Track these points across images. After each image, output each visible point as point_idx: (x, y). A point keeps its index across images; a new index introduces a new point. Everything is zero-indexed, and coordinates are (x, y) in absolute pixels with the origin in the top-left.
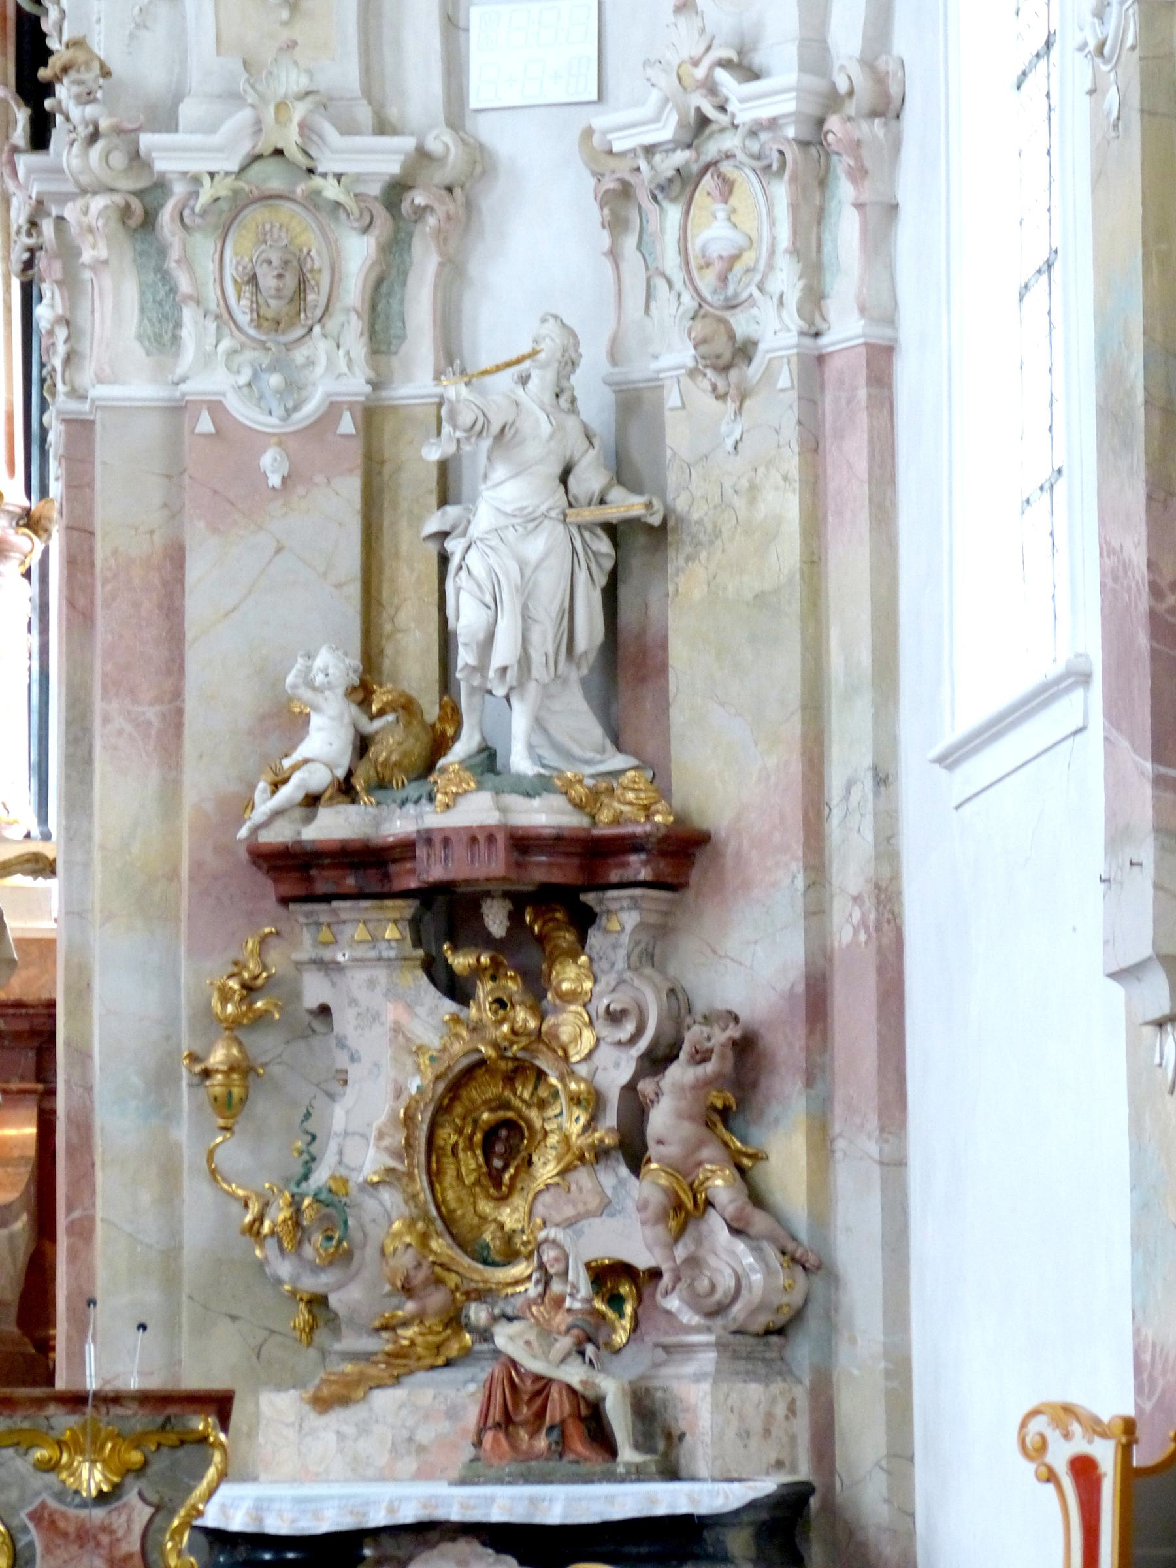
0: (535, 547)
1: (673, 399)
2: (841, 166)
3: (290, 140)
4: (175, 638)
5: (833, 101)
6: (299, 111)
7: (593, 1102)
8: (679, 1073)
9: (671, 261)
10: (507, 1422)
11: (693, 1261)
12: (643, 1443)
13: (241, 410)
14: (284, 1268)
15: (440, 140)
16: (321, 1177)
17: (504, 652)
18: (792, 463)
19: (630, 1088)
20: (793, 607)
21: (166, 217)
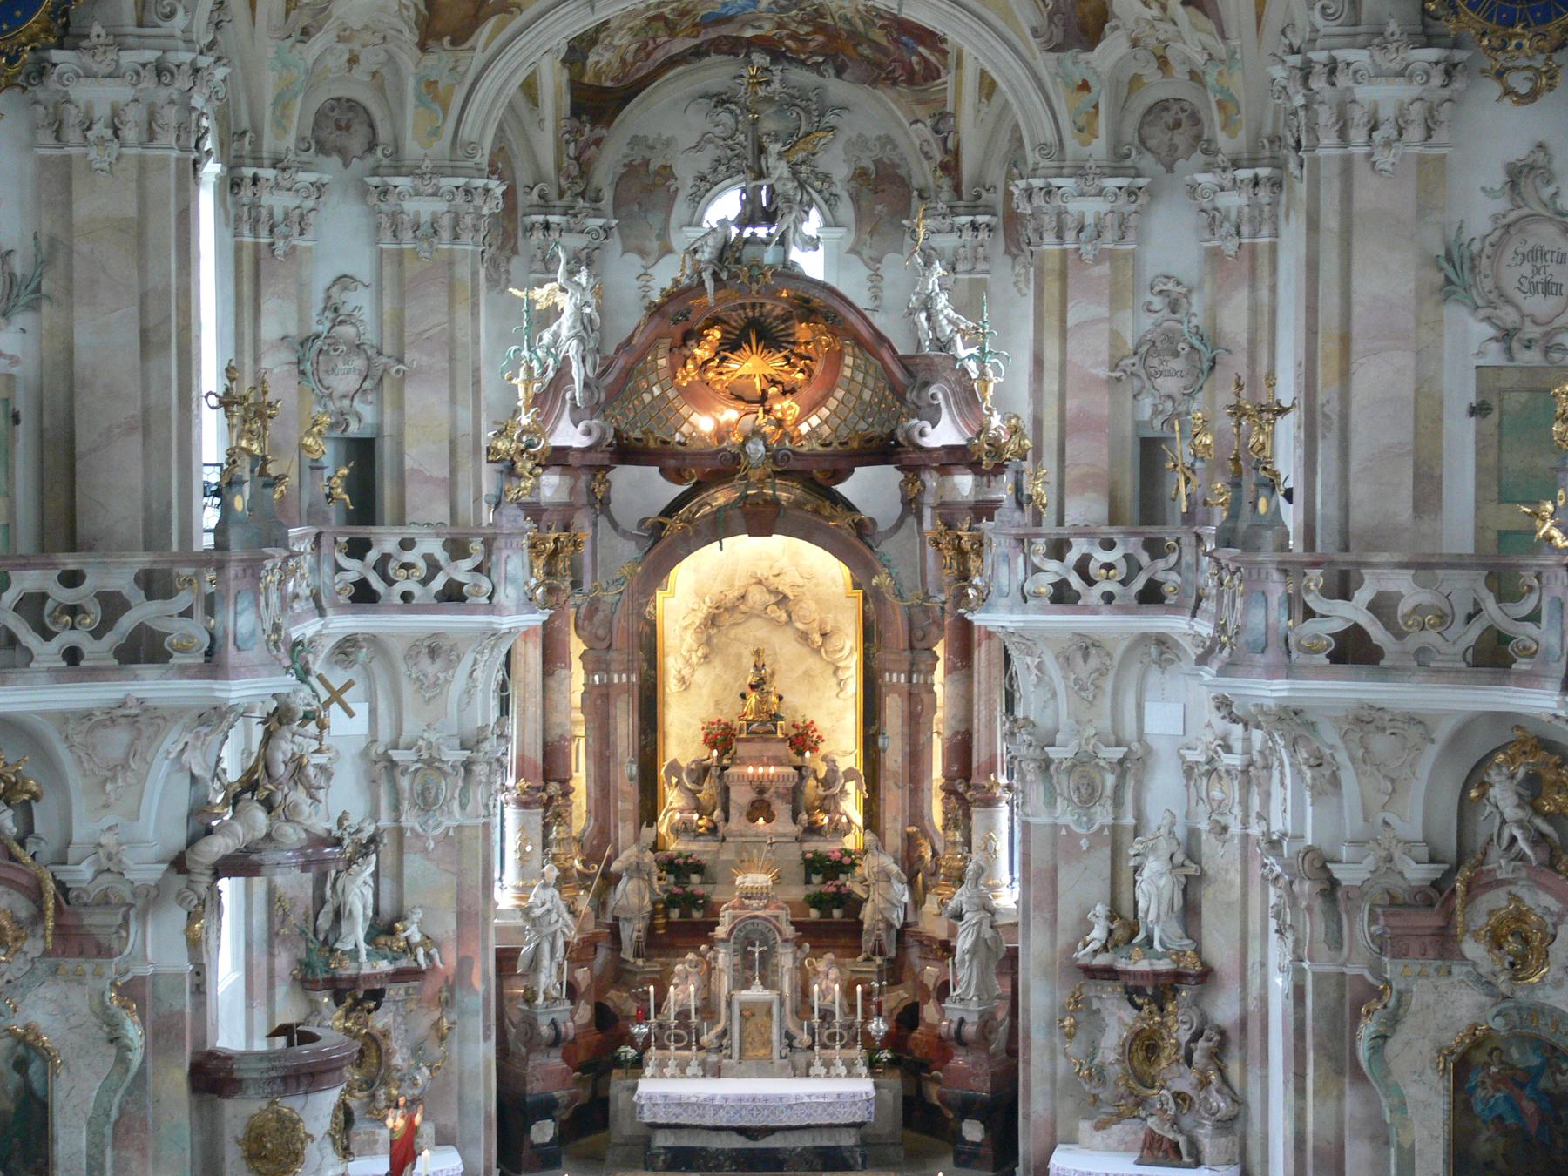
0: (1162, 882)
1: (1204, 837)
2: (1254, 781)
3: (1090, 749)
4: (1054, 893)
5: (1251, 763)
6: (1093, 741)
7: (1178, 1045)
8: (1202, 1043)
9: (1204, 795)
10: (1150, 1148)
11: (1206, 1098)
12: (1190, 1154)
13: (1074, 827)
14: (1087, 1087)
15: (1135, 746)
16: (1096, 1061)
17: (1152, 916)
18: (1238, 866)
19: (1189, 1042)
20: (1238, 908)
21: (1053, 768)
